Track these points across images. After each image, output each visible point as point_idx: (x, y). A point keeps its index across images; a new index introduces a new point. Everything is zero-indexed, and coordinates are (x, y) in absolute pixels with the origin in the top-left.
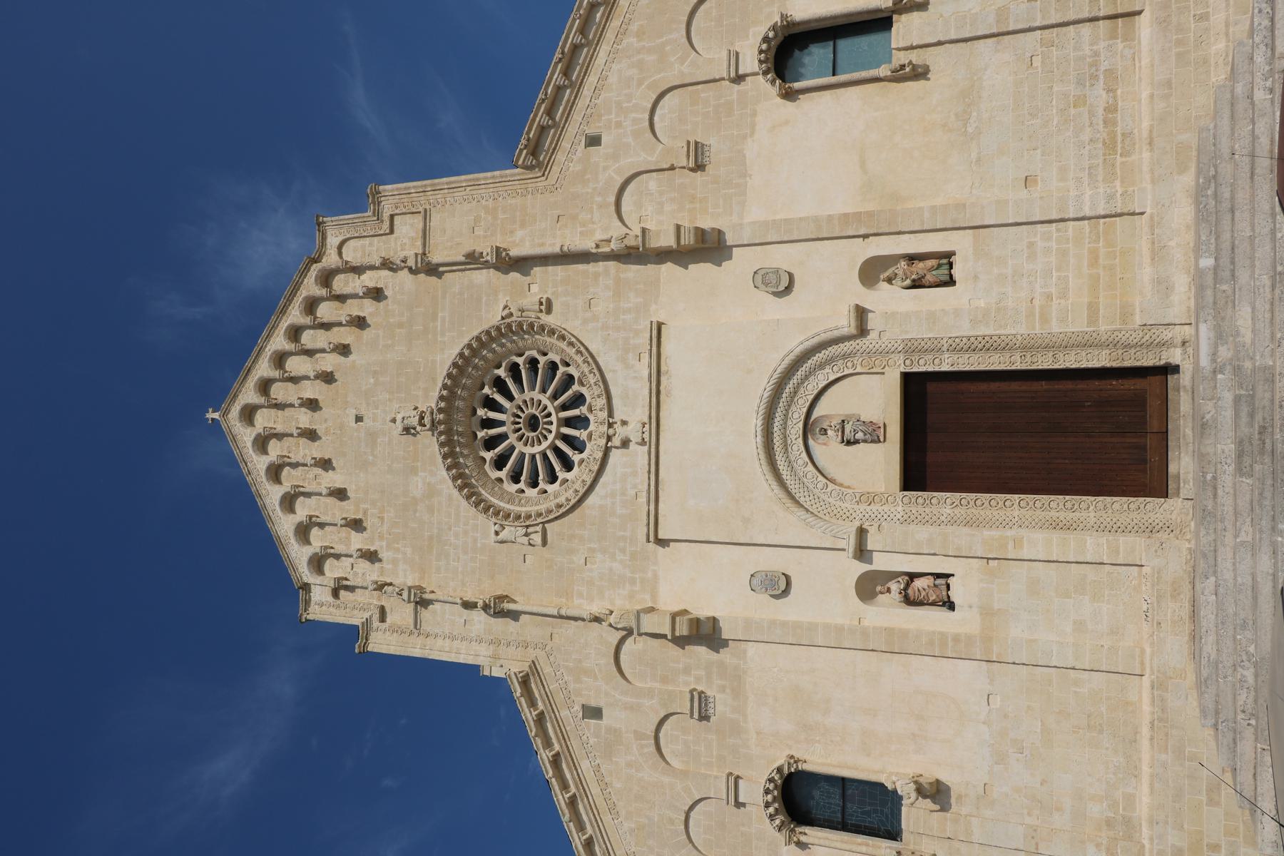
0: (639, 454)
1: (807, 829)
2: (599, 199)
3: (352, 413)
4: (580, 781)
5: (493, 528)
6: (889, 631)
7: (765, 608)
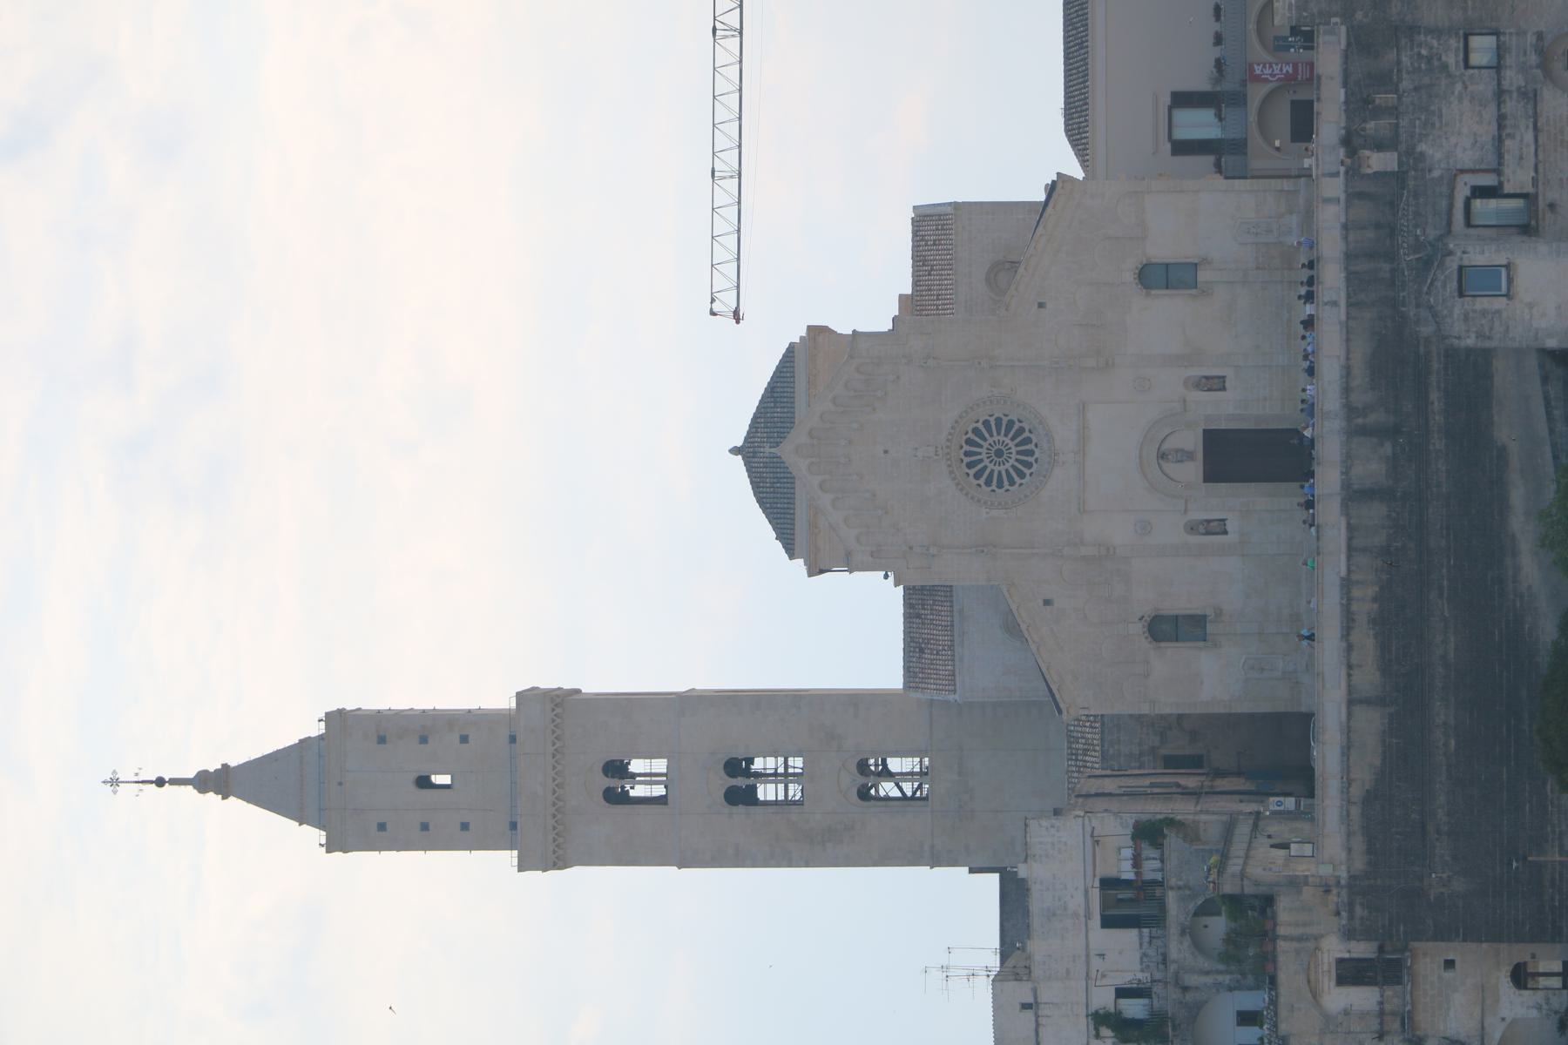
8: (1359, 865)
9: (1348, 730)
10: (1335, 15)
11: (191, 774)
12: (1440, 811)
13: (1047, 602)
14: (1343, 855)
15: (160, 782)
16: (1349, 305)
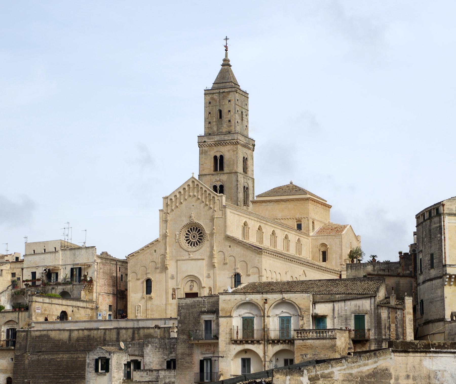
0: (187, 257)
1: (145, 283)
2: (222, 248)
3: (194, 204)
4: (146, 250)
5: (178, 233)
6: (168, 292)
7: (169, 276)
8: (33, 334)
9: (64, 330)
10: (180, 318)
11: (229, 57)
12: (44, 356)
13: (155, 251)
14: (35, 329)
15: (226, 50)
16: (164, 328)
